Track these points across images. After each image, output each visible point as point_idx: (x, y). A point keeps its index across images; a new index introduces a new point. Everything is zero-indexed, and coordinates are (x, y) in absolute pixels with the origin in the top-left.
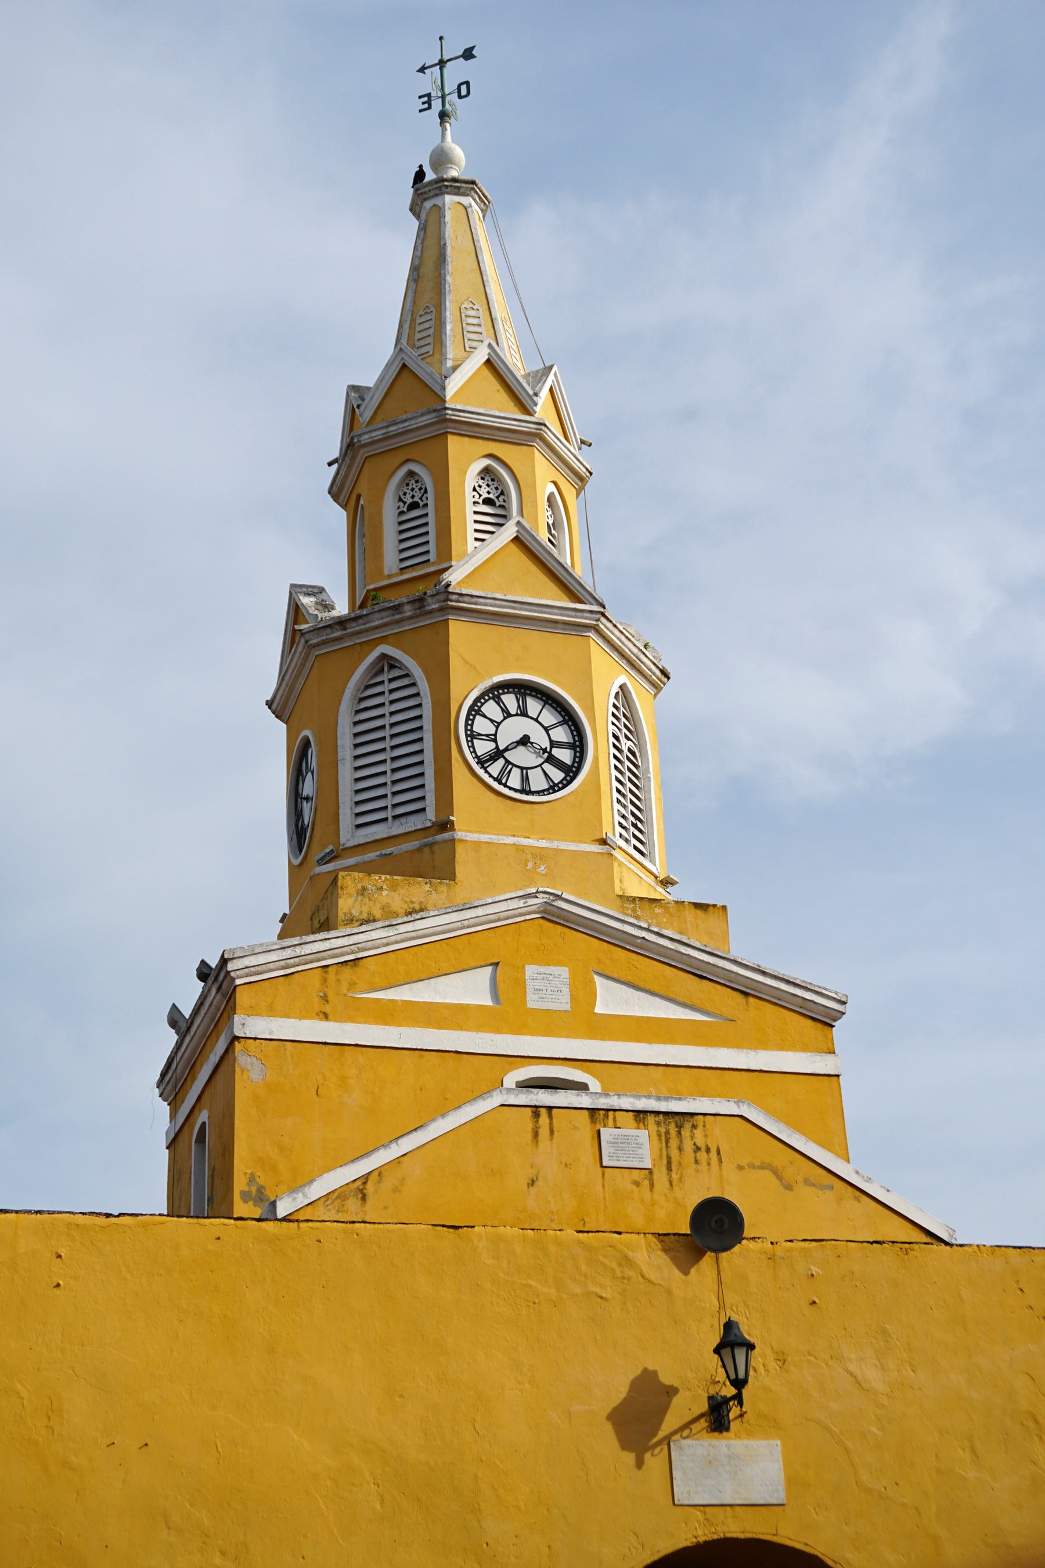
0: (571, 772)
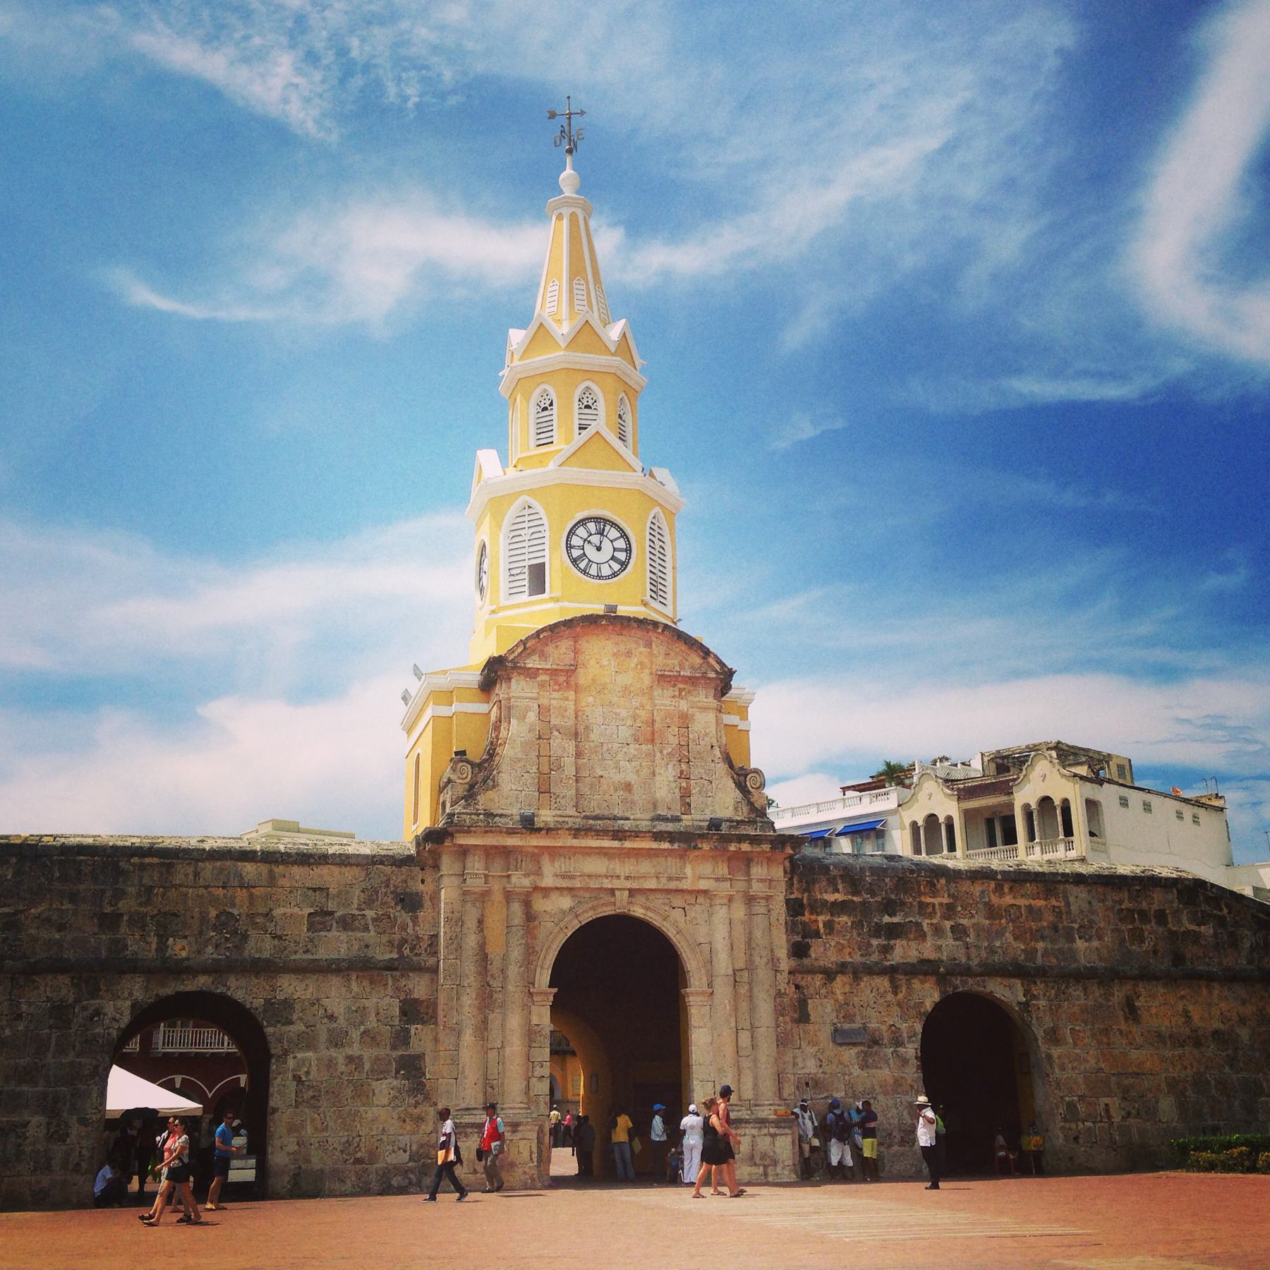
0: (624, 565)
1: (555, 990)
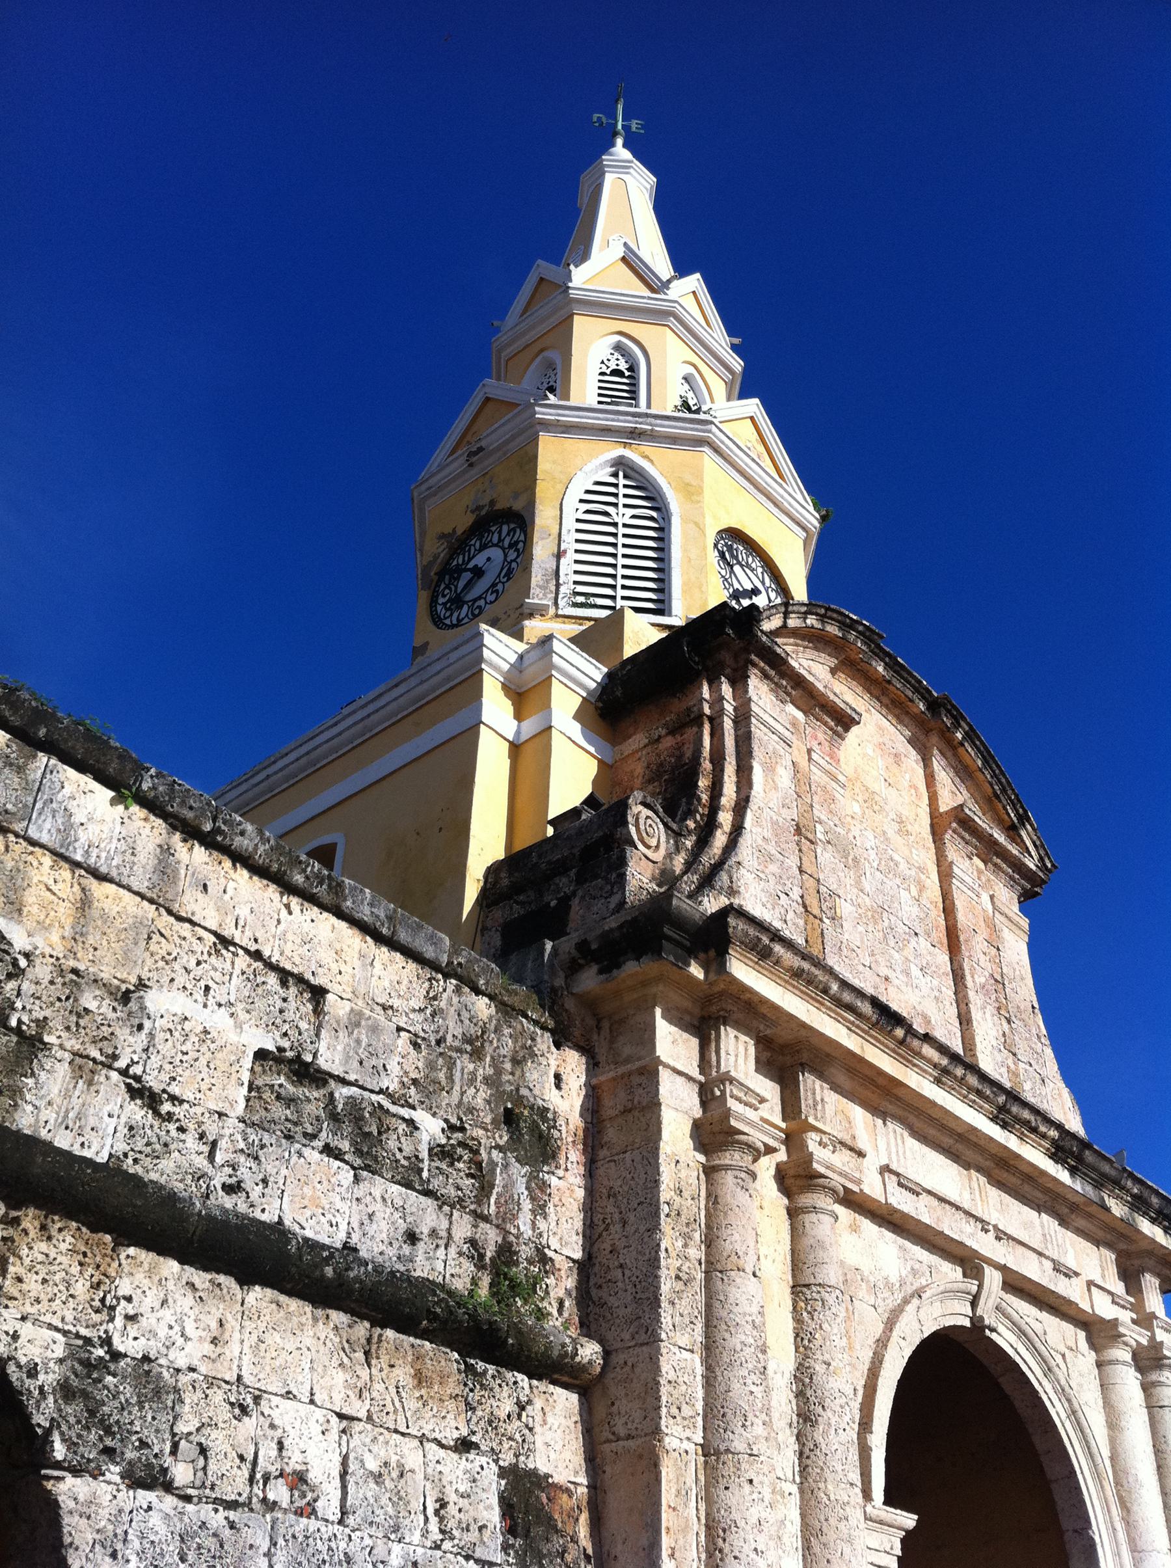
1: (909, 1520)
